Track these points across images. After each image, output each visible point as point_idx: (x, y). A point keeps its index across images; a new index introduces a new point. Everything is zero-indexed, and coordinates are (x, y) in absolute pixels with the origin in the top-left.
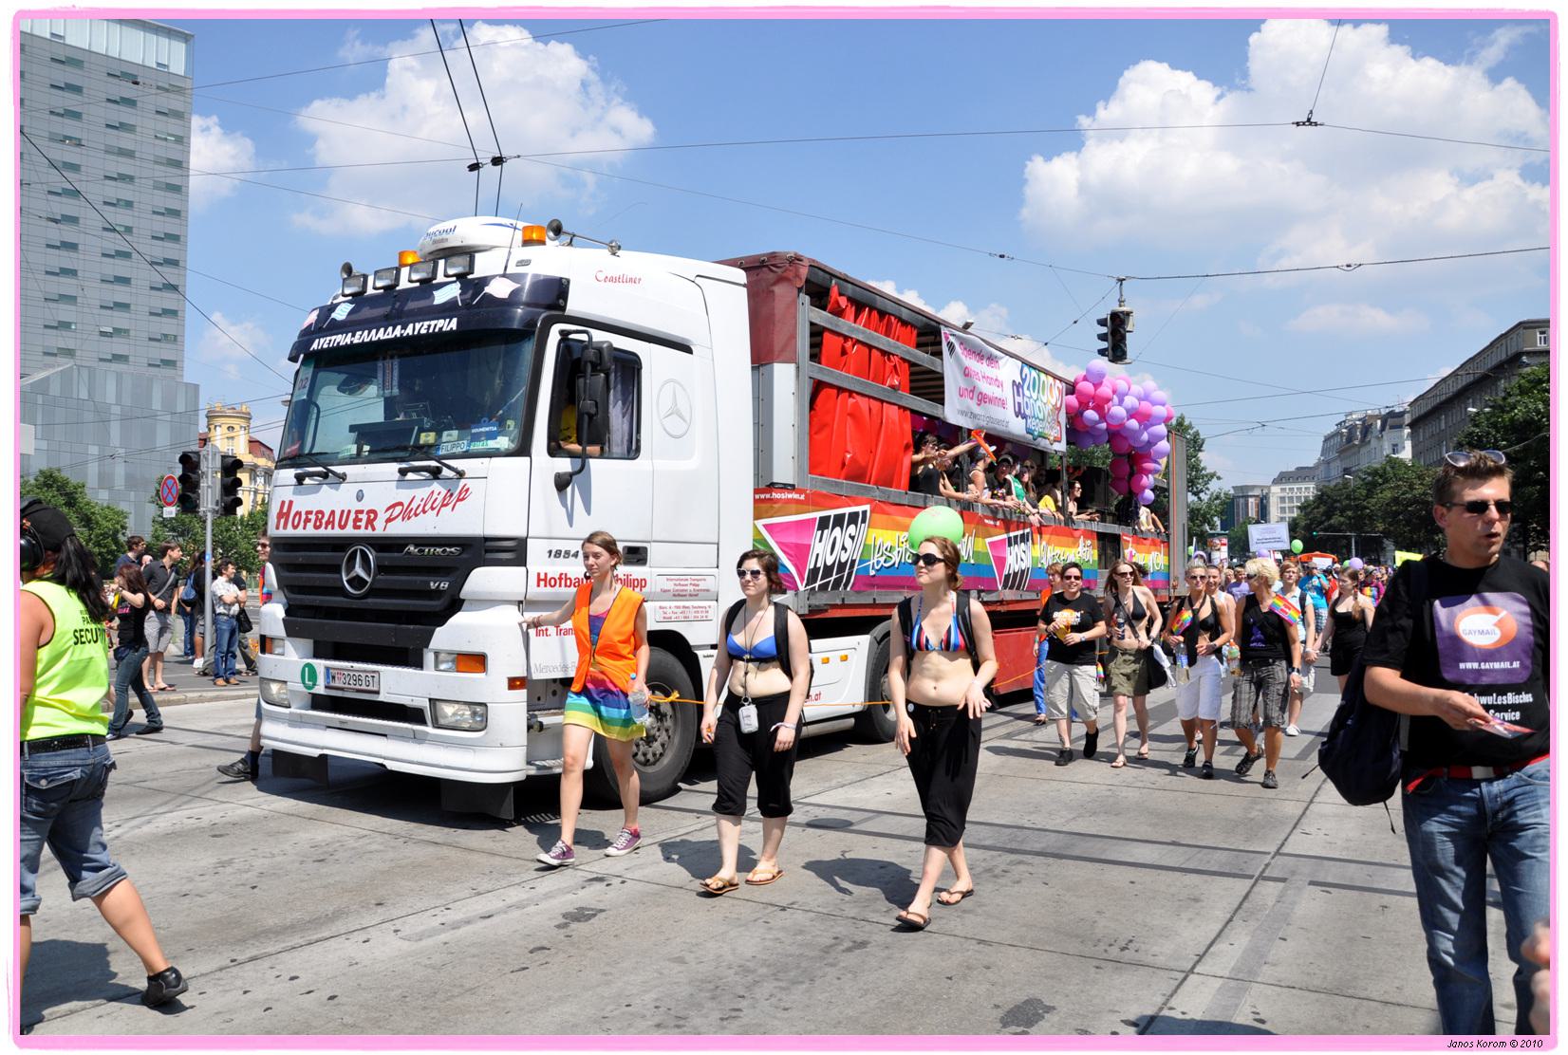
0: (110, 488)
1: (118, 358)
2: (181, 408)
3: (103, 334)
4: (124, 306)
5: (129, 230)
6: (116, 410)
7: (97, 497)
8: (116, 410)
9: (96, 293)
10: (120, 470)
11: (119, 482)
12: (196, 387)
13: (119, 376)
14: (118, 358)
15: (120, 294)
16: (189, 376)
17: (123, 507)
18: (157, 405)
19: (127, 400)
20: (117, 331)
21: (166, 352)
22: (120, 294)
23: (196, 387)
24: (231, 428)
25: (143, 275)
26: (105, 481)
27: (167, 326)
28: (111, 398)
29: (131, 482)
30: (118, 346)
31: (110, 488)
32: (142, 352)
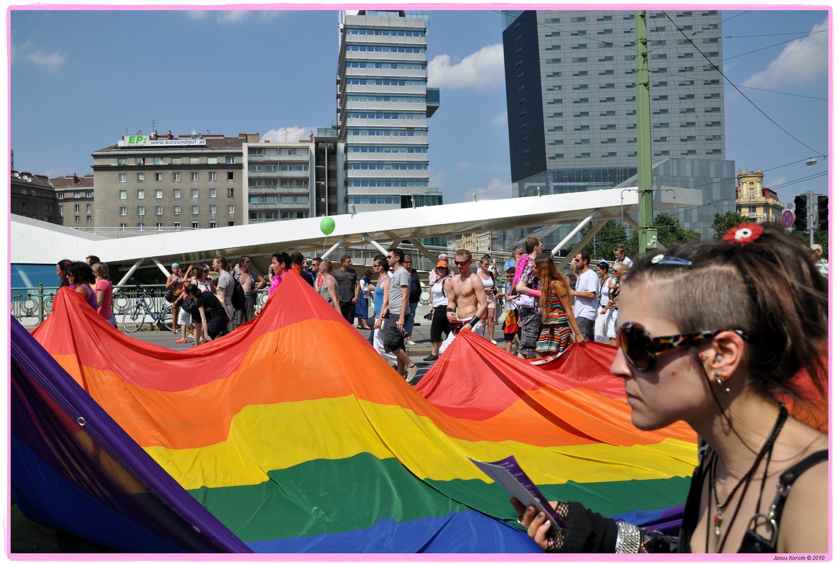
0: (690, 222)
1: (691, 152)
2: (725, 175)
3: (682, 140)
4: (692, 124)
5: (692, 83)
6: (691, 180)
7: (686, 227)
8: (691, 180)
9: (675, 119)
10: (695, 213)
11: (695, 219)
12: (733, 162)
13: (692, 161)
14: (691, 152)
15: (690, 118)
16: (728, 157)
17: (697, 230)
18: (712, 175)
19: (697, 174)
20: (690, 138)
21: (715, 145)
22: (690, 118)
23: (733, 162)
24: (752, 183)
25: (700, 105)
26: (688, 218)
27: (715, 131)
28: (689, 174)
29: (701, 217)
30: (690, 146)
31: (690, 222)
32: (702, 147)
